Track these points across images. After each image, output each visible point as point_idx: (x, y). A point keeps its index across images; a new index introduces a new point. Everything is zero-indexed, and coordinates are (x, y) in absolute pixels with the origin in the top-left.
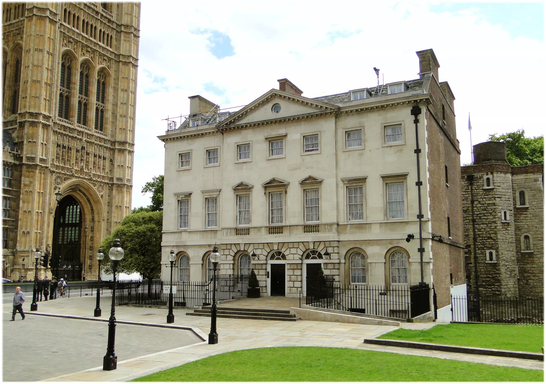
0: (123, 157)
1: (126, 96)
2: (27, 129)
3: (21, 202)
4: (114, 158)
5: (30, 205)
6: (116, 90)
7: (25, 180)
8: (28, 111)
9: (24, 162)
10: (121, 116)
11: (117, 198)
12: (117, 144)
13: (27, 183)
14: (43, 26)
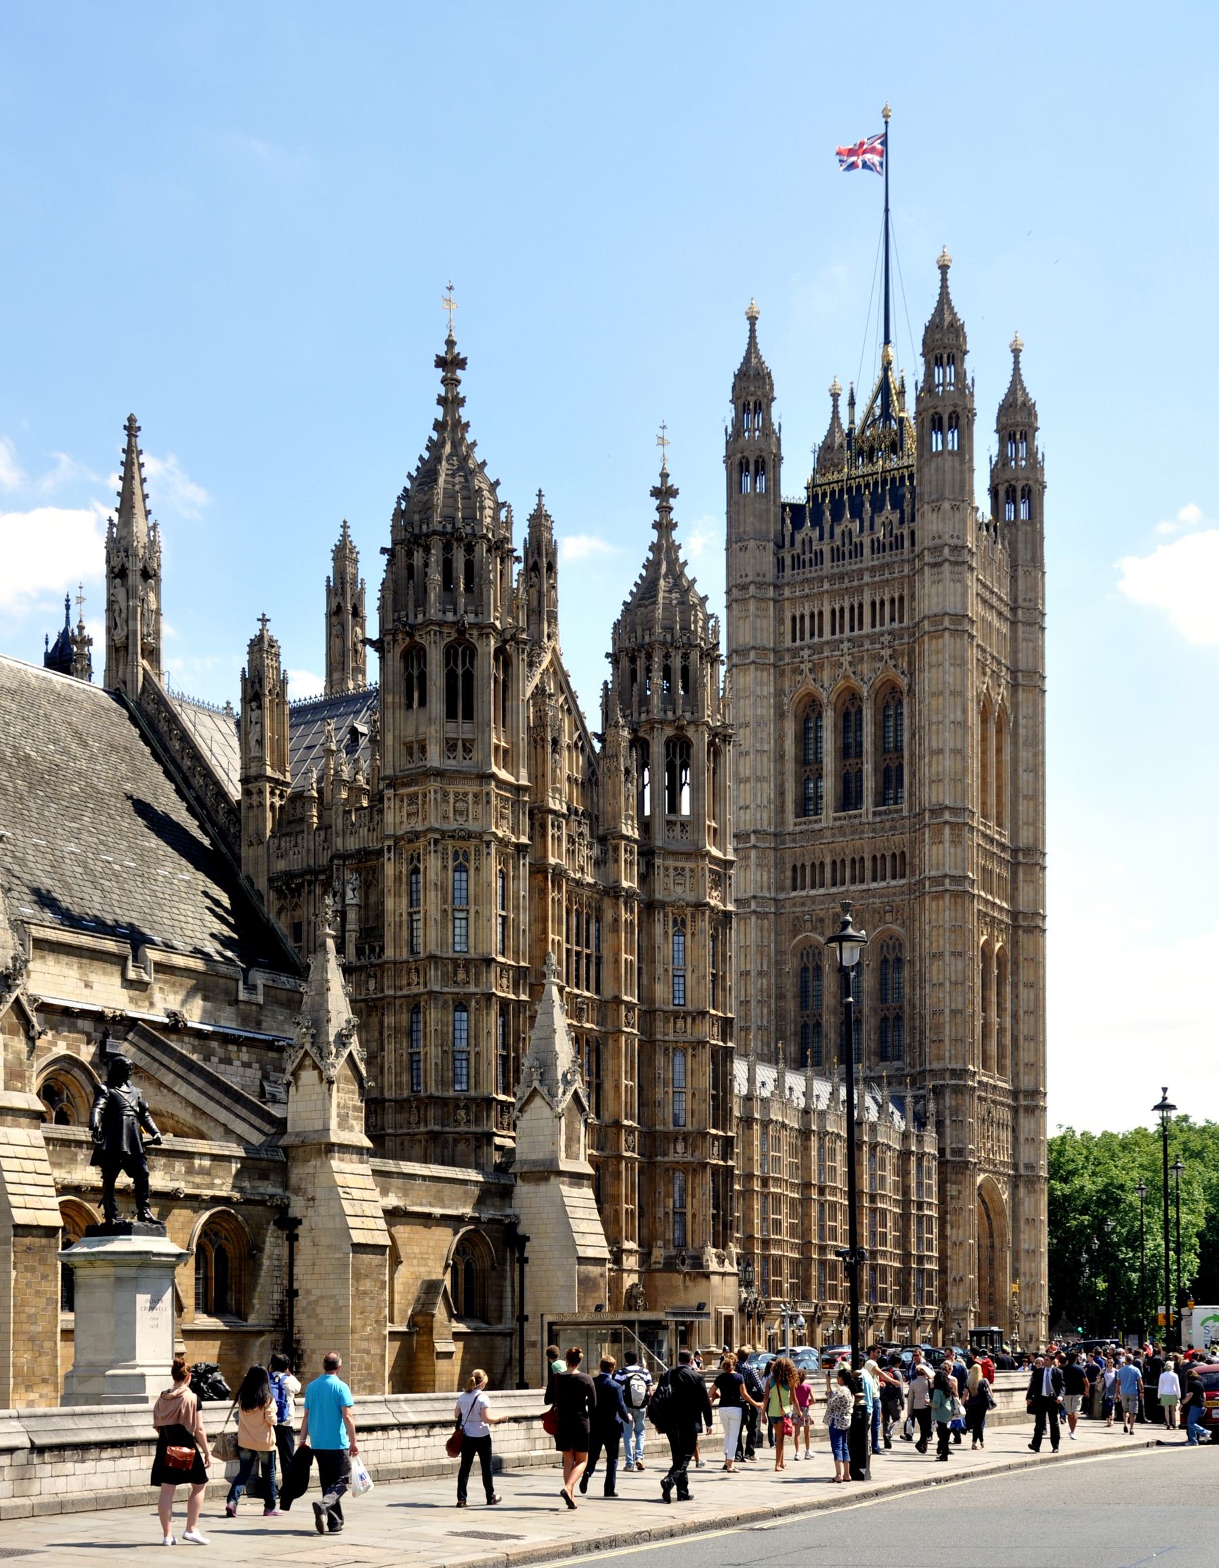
0: (1032, 1121)
1: (1032, 998)
2: (949, 1100)
3: (949, 1227)
4: (1017, 1123)
5: (961, 1231)
6: (1015, 985)
7: (952, 1189)
8: (950, 1067)
9: (949, 1157)
10: (1026, 1039)
11: (1026, 1204)
12: (1021, 1096)
13: (954, 1193)
14: (959, 908)
